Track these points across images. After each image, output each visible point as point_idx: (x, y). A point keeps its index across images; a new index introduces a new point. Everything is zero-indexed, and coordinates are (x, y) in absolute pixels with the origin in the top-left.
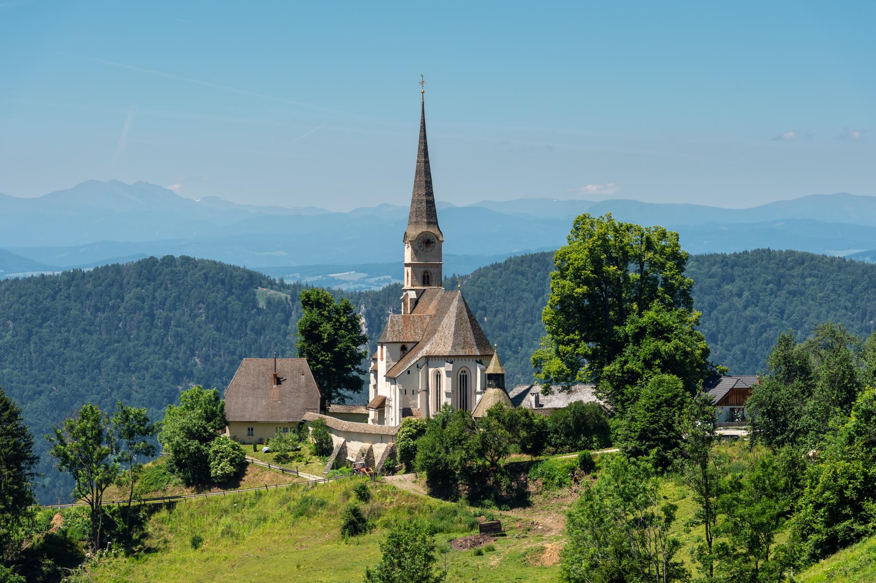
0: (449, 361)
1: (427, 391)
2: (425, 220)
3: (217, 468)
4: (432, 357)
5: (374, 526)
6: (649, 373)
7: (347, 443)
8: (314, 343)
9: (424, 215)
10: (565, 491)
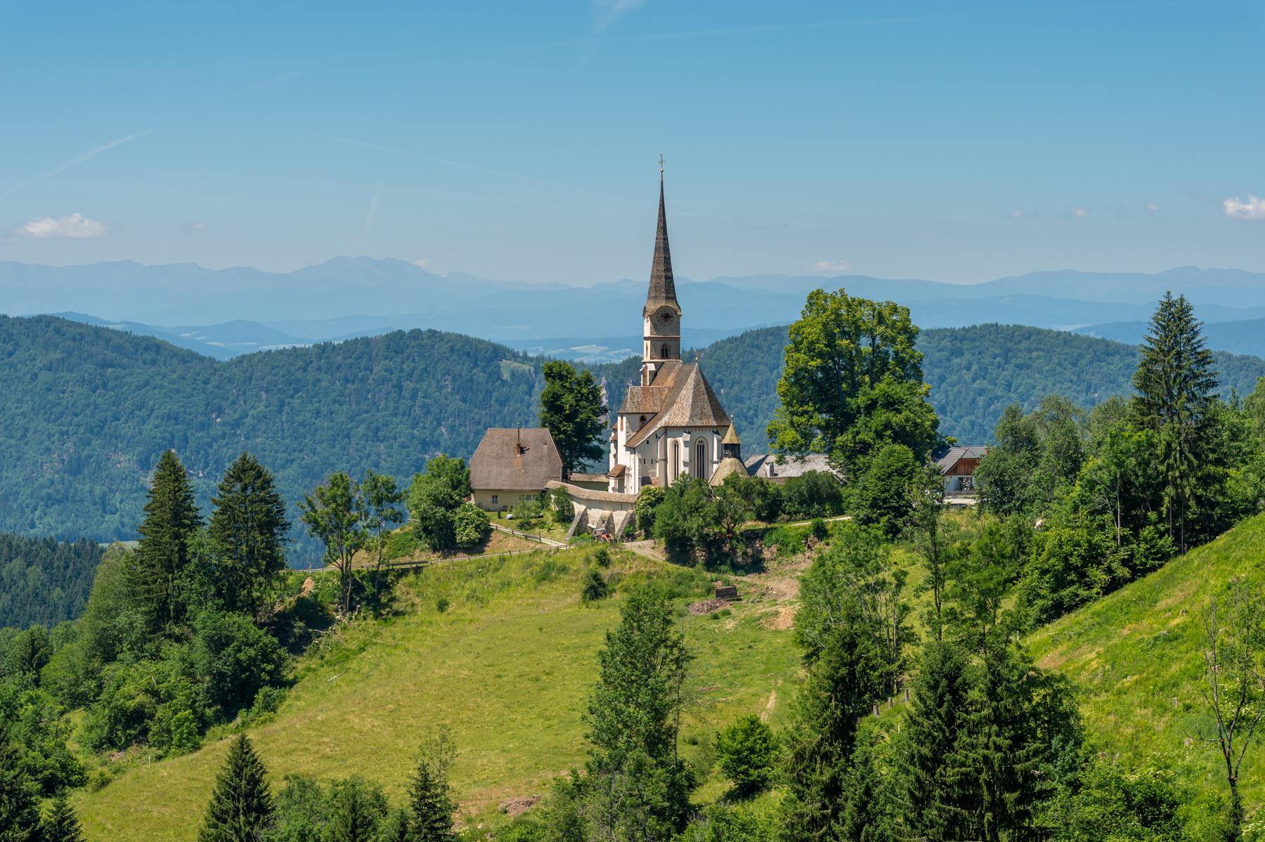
1: (666, 460)
5: (614, 591)
8: (556, 414)
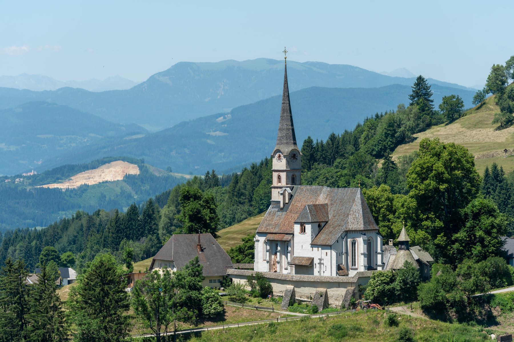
0: (363, 234)
1: (347, 253)
2: (292, 142)
3: (210, 308)
6: (488, 238)
7: (295, 288)
8: (199, 223)
9: (291, 138)
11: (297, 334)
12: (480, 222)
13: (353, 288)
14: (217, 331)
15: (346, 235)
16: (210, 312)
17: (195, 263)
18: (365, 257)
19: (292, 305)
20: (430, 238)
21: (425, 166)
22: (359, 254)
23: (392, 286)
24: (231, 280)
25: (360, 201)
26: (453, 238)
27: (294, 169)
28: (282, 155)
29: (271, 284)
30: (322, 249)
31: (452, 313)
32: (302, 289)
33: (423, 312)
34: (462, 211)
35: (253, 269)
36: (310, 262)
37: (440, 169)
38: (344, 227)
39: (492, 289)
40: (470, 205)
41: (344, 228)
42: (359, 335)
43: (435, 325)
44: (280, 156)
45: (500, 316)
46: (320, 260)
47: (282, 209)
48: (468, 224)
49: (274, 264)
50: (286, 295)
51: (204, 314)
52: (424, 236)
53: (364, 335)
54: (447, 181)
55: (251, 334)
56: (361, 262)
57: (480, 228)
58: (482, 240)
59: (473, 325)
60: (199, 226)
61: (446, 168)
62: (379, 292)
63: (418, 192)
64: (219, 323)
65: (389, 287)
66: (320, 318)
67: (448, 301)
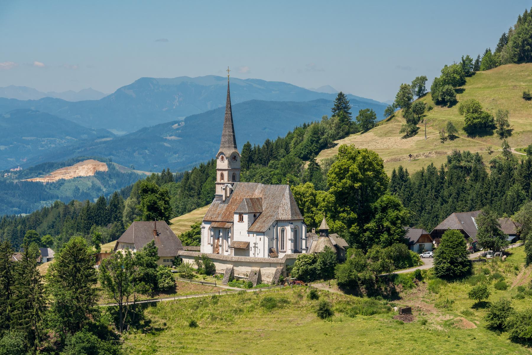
1: (277, 238)
2: (233, 146)
4: (280, 220)
9: (233, 143)
10: (414, 290)
11: (235, 305)
12: (387, 214)
13: (282, 268)
14: (169, 302)
15: (277, 224)
16: (164, 285)
17: (151, 245)
18: (292, 242)
19: (231, 281)
20: (346, 227)
21: (343, 168)
22: (288, 240)
23: (314, 266)
24: (182, 259)
25: (289, 196)
26: (365, 228)
27: (235, 169)
28: (225, 157)
29: (214, 263)
30: (257, 235)
31: (363, 289)
32: (240, 267)
33: (339, 288)
34: (373, 205)
35: (199, 251)
36: (246, 246)
37: (355, 170)
38: (275, 217)
39: (395, 269)
40: (379, 200)
41: (275, 218)
42: (286, 306)
43: (348, 299)
44: (222, 158)
45: (402, 292)
46: (255, 244)
47: (224, 202)
48: (377, 216)
49: (217, 247)
50: (226, 273)
51: (158, 287)
52: (341, 225)
53: (290, 306)
54: (361, 180)
55: (196, 304)
56: (289, 246)
57: (387, 219)
58: (388, 230)
59: (380, 299)
60: (156, 215)
61: (360, 169)
62: (303, 271)
63: (336, 189)
64: (171, 295)
65: (311, 267)
66: (254, 292)
67: (359, 279)
